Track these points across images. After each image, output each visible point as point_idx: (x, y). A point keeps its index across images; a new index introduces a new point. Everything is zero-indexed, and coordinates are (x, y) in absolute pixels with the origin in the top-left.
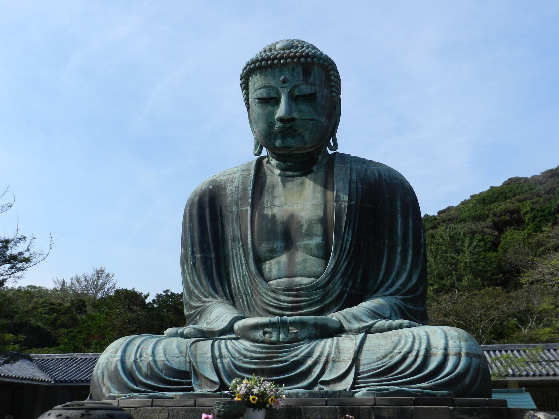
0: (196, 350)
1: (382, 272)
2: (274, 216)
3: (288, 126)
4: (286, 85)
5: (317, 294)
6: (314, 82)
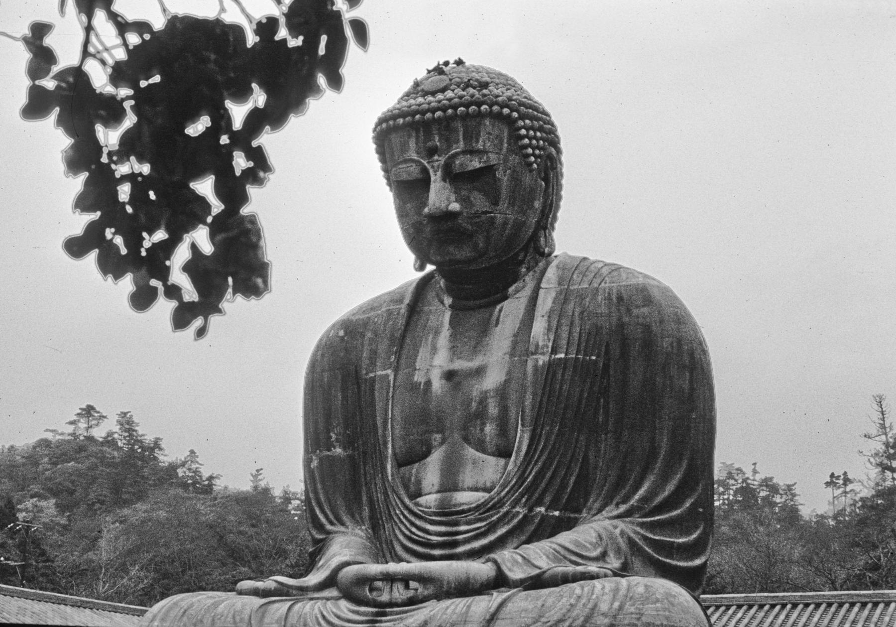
0: (263, 616)
2: (428, 383)
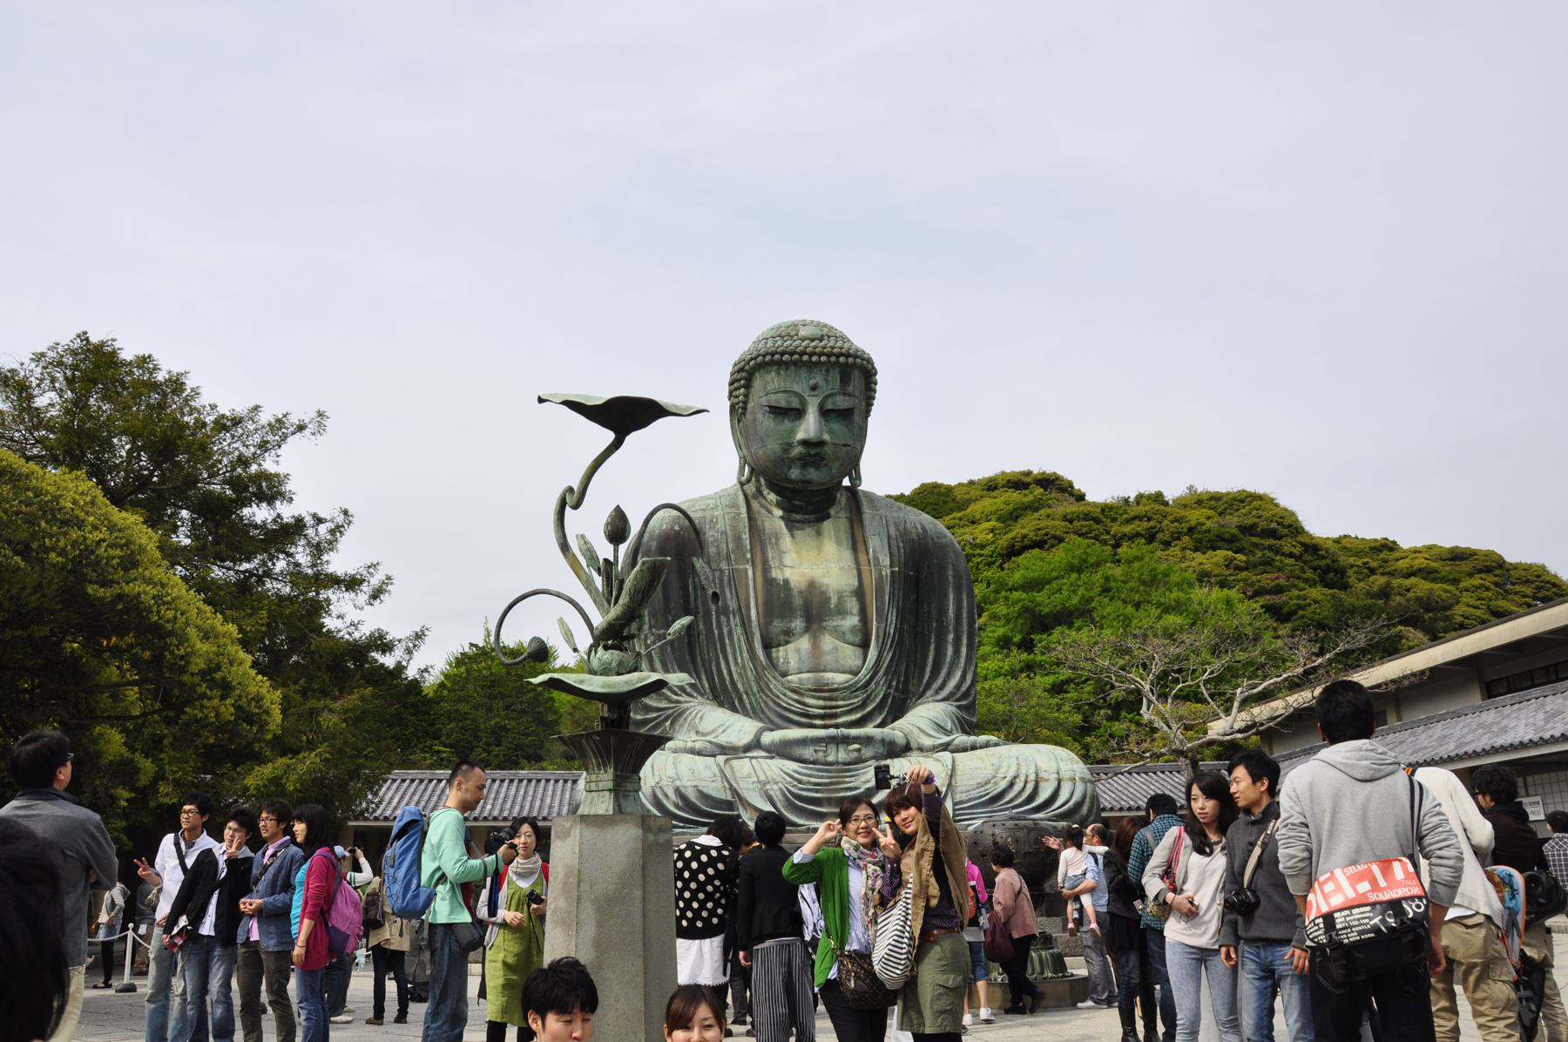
0: (733, 773)
1: (929, 669)
2: (786, 582)
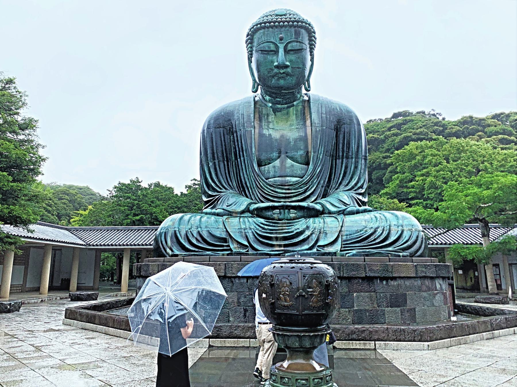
2: (270, 135)
3: (282, 71)
4: (283, 41)
5: (301, 188)
6: (302, 40)
